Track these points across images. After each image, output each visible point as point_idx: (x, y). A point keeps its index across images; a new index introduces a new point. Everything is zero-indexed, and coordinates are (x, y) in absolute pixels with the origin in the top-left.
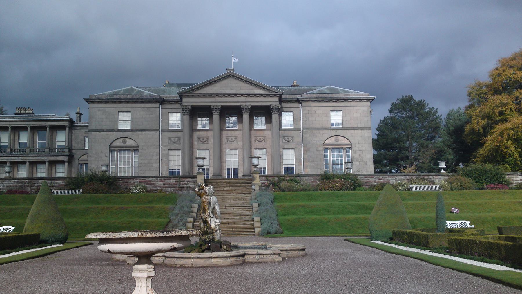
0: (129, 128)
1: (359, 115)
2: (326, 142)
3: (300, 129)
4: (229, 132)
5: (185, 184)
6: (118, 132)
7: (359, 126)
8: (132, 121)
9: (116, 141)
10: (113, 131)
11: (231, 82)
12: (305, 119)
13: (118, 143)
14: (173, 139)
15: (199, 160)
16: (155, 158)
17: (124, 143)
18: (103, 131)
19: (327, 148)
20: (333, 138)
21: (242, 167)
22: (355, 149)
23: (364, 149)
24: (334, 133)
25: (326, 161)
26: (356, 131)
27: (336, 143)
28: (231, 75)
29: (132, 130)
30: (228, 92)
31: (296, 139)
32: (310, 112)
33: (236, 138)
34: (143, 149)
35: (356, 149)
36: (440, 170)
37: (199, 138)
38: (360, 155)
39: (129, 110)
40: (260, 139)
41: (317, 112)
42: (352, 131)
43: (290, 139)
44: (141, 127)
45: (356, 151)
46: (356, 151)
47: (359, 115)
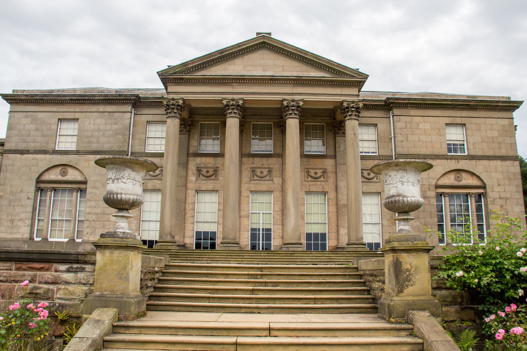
0: (73, 147)
1: (495, 134)
2: (442, 182)
4: (257, 160)
8: (79, 136)
10: (45, 152)
12: (399, 138)
13: (54, 175)
17: (64, 176)
18: (28, 152)
19: (441, 195)
20: (452, 176)
21: (280, 227)
22: (492, 194)
23: (508, 195)
24: (453, 165)
26: (493, 163)
27: (456, 183)
28: (264, 44)
29: (77, 152)
30: (258, 72)
32: (408, 126)
33: (270, 171)
34: (94, 187)
37: (199, 170)
40: (316, 173)
41: (421, 126)
42: (486, 162)
45: (494, 199)
46: (494, 199)
47: (495, 134)
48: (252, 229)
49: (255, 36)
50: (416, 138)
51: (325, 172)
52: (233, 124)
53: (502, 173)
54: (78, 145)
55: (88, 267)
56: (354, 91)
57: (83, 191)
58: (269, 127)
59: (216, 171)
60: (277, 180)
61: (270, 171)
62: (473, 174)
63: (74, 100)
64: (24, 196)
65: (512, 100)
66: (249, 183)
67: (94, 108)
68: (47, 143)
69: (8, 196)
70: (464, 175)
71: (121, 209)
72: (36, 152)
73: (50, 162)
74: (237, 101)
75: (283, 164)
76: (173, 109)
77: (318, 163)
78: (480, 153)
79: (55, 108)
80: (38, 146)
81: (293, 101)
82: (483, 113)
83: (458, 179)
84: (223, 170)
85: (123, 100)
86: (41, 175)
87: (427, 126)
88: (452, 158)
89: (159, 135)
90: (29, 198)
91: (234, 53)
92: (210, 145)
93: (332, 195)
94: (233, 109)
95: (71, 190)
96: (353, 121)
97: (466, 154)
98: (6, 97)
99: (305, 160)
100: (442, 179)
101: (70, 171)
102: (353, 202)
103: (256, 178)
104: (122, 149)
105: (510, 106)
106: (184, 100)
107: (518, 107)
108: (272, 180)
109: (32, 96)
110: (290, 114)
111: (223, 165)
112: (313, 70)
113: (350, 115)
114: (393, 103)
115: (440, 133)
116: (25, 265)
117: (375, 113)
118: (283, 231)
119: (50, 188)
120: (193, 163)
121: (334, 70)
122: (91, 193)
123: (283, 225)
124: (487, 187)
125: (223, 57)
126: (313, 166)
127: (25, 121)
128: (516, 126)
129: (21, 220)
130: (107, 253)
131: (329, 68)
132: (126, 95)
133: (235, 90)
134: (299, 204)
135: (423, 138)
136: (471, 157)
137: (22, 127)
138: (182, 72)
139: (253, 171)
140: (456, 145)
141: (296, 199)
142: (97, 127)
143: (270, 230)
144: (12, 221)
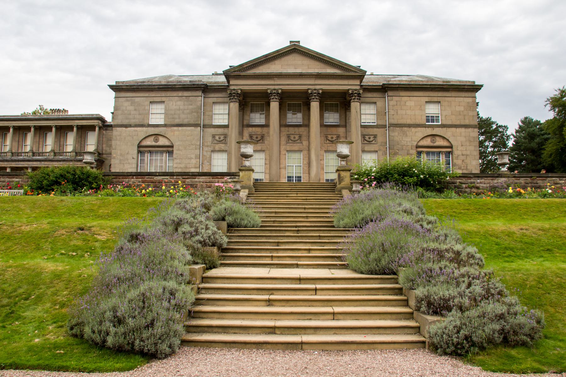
0: (162, 122)
1: (462, 109)
2: (421, 143)
4: (291, 129)
6: (149, 128)
8: (166, 114)
9: (147, 139)
10: (142, 126)
12: (392, 112)
14: (217, 138)
17: (156, 142)
18: (130, 126)
21: (307, 175)
22: (456, 152)
23: (468, 153)
24: (429, 131)
26: (459, 130)
27: (432, 144)
28: (295, 49)
29: (165, 126)
30: (291, 70)
31: (380, 139)
32: (398, 104)
33: (300, 137)
34: (179, 150)
35: (459, 153)
38: (463, 161)
39: (163, 99)
42: (453, 129)
43: (371, 139)
44: (177, 121)
45: (458, 156)
46: (458, 156)
47: (462, 109)
48: (288, 177)
49: (289, 44)
50: (404, 112)
51: (338, 137)
52: (274, 106)
53: (465, 137)
54: (165, 120)
55: (237, 177)
56: (358, 82)
57: (171, 153)
58: (299, 105)
59: (263, 137)
60: (305, 143)
61: (300, 137)
62: (444, 138)
63: (160, 88)
64: (130, 157)
65: (476, 84)
66: (286, 145)
67: (175, 94)
68: (143, 119)
69: (119, 157)
70: (437, 138)
71: (246, 158)
72: (136, 126)
73: (146, 132)
74: (277, 90)
75: (309, 132)
76: (234, 96)
77: (334, 130)
78: (449, 123)
79: (147, 94)
80: (137, 121)
81: (315, 90)
83: (433, 141)
84: (269, 136)
85: (196, 87)
86: (140, 142)
88: (429, 126)
89: (222, 112)
90: (133, 158)
91: (274, 56)
92: (258, 118)
94: (274, 96)
95: (162, 152)
96: (356, 103)
97: (440, 123)
98: (112, 87)
99: (325, 128)
100: (421, 141)
101: (161, 139)
102: (355, 157)
103: (290, 141)
104: (197, 123)
105: (474, 88)
106: (241, 90)
107: (480, 89)
108: (302, 143)
109: (131, 86)
110: (313, 99)
111: (268, 133)
112: (329, 67)
113: (354, 99)
114: (388, 87)
115: (422, 109)
116: (215, 177)
117: (375, 95)
118: (309, 178)
119: (147, 151)
120: (247, 132)
121: (343, 67)
122: (176, 154)
123: (309, 174)
124: (454, 147)
125: (267, 59)
126: (330, 133)
127: (126, 104)
128: (478, 103)
130: (244, 172)
131: (340, 66)
132: (198, 85)
133: (276, 83)
134: (320, 160)
135: (409, 112)
136: (443, 126)
137: (124, 108)
138: (239, 71)
139: (289, 137)
140: (433, 117)
141: (317, 156)
142: (178, 107)
143: (300, 177)
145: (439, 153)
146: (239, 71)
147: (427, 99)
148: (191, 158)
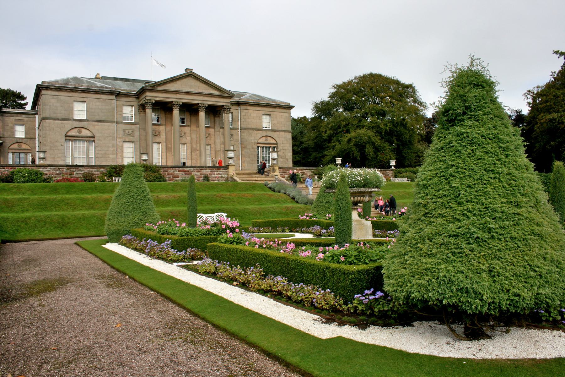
0: (84, 118)
2: (260, 141)
3: (237, 129)
5: (219, 174)
7: (283, 129)
10: (68, 120)
11: (190, 81)
12: (243, 120)
13: (74, 133)
14: (127, 132)
15: (229, 152)
16: (111, 149)
18: (58, 119)
20: (264, 138)
23: (286, 148)
24: (265, 134)
25: (258, 157)
27: (266, 142)
28: (190, 75)
29: (87, 121)
34: (99, 140)
36: (391, 167)
41: (252, 115)
42: (278, 133)
44: (97, 118)
50: (250, 120)
78: (276, 129)
82: (278, 110)
83: (266, 140)
87: (255, 115)
93: (213, 146)
105: (291, 107)
127: (53, 101)
129: (59, 157)
135: (253, 120)
144: (54, 158)
145: (269, 147)
146: (153, 86)
147: (263, 112)
148: (109, 147)
